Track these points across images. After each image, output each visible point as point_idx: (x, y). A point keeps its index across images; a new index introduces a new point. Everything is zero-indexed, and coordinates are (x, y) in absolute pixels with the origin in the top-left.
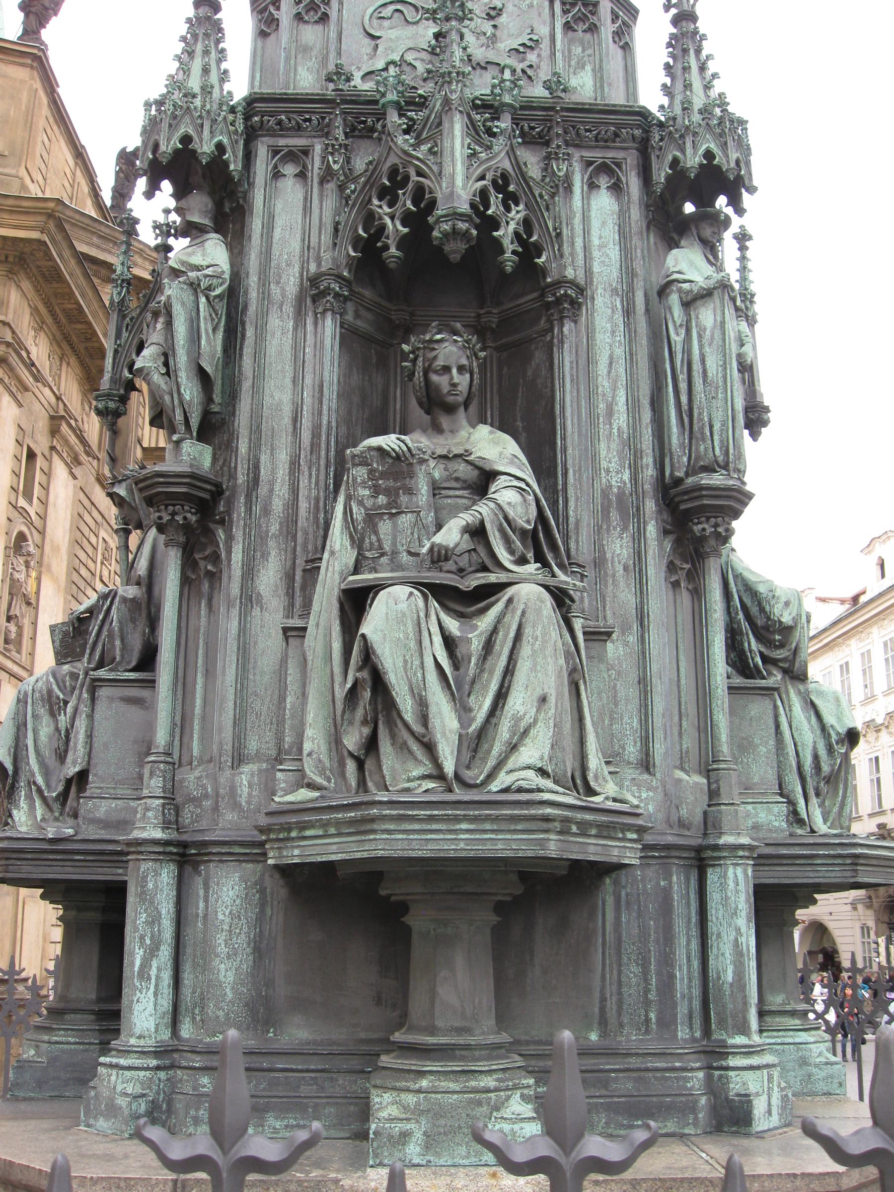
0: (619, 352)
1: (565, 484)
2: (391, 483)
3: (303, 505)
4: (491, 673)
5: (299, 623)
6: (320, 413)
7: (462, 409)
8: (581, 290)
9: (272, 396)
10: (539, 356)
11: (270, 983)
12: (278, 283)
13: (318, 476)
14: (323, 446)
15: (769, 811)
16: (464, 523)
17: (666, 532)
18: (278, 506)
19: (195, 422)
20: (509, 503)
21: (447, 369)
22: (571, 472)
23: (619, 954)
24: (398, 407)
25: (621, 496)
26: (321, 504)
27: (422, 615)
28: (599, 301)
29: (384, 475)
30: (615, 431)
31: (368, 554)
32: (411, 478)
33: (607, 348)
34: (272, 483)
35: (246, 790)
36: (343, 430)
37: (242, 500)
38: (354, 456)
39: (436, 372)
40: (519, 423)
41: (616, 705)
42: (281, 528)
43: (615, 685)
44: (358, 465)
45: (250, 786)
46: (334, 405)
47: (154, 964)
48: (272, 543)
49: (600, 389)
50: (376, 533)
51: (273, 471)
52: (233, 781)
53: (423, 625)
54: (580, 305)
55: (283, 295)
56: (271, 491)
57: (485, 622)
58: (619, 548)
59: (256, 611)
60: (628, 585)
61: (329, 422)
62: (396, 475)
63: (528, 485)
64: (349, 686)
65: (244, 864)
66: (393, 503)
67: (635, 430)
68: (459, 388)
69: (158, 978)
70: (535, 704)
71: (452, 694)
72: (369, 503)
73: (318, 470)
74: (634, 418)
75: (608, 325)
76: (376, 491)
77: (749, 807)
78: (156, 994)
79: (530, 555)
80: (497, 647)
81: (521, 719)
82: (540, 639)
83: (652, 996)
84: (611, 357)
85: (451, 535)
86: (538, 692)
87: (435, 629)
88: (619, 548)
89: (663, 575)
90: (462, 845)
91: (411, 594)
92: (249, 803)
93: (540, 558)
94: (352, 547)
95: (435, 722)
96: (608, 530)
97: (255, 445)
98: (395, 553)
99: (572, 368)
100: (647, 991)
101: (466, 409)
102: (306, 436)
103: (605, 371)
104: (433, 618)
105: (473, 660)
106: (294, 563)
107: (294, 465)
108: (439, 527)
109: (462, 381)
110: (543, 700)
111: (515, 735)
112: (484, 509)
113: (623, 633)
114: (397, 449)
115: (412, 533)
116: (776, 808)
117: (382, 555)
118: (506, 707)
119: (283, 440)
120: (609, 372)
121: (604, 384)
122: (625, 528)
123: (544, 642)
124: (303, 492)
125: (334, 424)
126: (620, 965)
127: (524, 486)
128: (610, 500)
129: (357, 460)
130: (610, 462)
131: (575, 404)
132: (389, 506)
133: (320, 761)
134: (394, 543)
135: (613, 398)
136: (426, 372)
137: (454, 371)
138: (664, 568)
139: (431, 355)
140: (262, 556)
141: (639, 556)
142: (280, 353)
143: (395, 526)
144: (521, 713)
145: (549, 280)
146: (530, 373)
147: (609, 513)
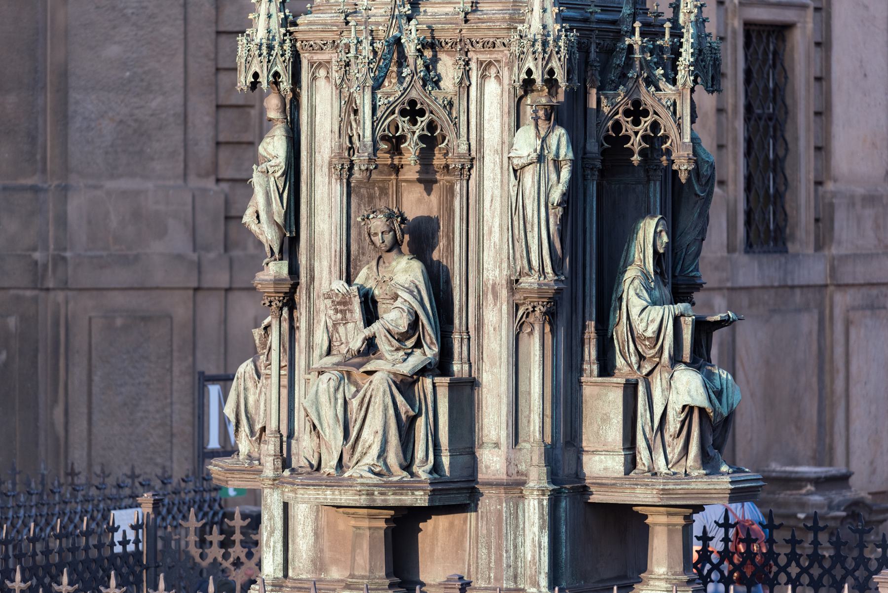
0: (497, 192)
2: (342, 307)
11: (321, 551)
15: (614, 460)
19: (276, 250)
23: (477, 543)
34: (321, 279)
47: (272, 539)
51: (321, 272)
56: (321, 284)
62: (344, 303)
66: (344, 318)
69: (274, 547)
72: (334, 318)
76: (337, 311)
77: (603, 457)
78: (273, 555)
83: (492, 565)
84: (492, 197)
86: (375, 429)
100: (490, 562)
116: (617, 458)
122: (495, 304)
126: (477, 548)
132: (342, 320)
134: (347, 338)
142: (322, 199)
143: (346, 329)
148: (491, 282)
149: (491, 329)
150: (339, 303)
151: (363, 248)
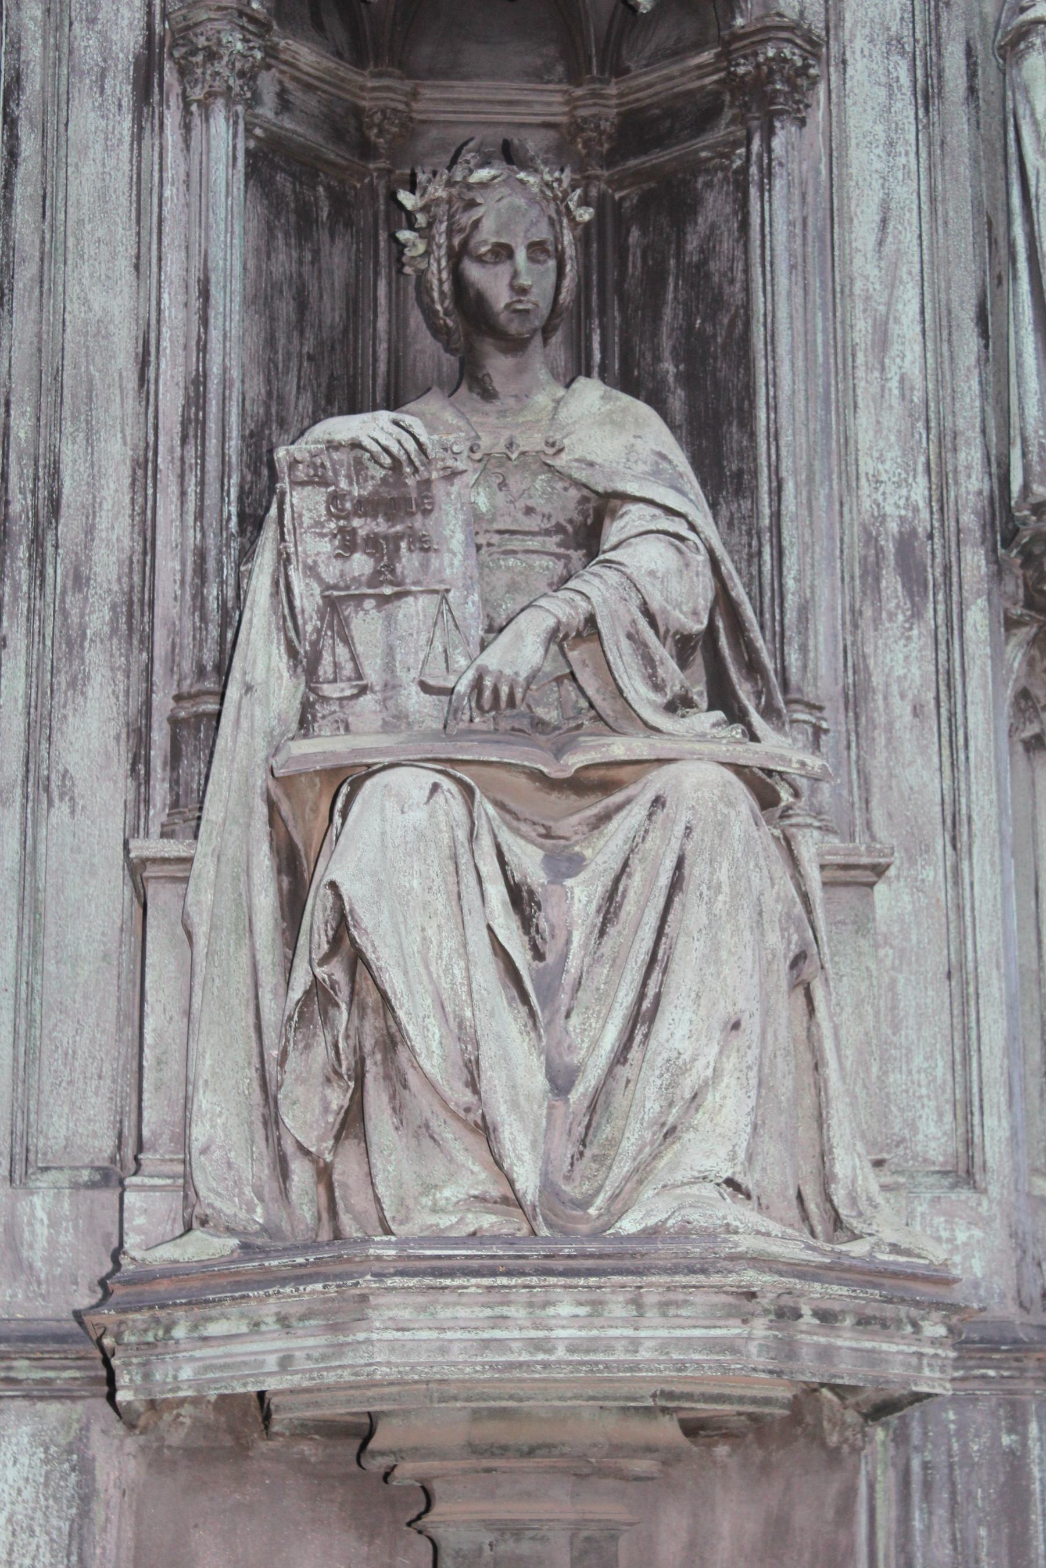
0: (905, 193)
1: (777, 516)
2: (381, 526)
3: (169, 568)
4: (617, 963)
5: (173, 848)
6: (203, 348)
7: (538, 340)
8: (814, 46)
9: (86, 301)
10: (715, 205)
12: (92, 21)
13: (201, 497)
14: (212, 426)
16: (551, 622)
17: (1011, 624)
18: (107, 566)
20: (652, 573)
21: (503, 252)
22: (789, 488)
24: (382, 323)
25: (906, 543)
26: (211, 565)
27: (462, 835)
28: (858, 69)
29: (366, 507)
30: (894, 384)
31: (327, 690)
32: (426, 513)
33: (877, 185)
34: (91, 511)
35: (43, 1231)
36: (256, 387)
37: (22, 552)
38: (294, 463)
39: (480, 259)
40: (669, 367)
41: (896, 1029)
42: (115, 619)
43: (893, 982)
44: (303, 484)
45: (54, 1223)
46: (235, 330)
48: (94, 655)
49: (858, 285)
50: (347, 641)
51: (93, 484)
52: (13, 1213)
53: (464, 859)
54: (814, 81)
55: (106, 53)
56: (90, 530)
57: (603, 853)
58: (901, 660)
59: (61, 811)
60: (923, 750)
61: (225, 370)
63: (692, 527)
64: (297, 994)
65: (40, 1406)
66: (385, 571)
67: (939, 382)
68: (532, 297)
70: (717, 1035)
71: (532, 1014)
72: (330, 572)
73: (202, 483)
74: (938, 354)
75: (879, 128)
76: (348, 543)
79: (699, 692)
80: (629, 908)
81: (684, 1070)
82: (726, 889)
85: (521, 652)
86: (724, 1010)
87: (490, 867)
88: (901, 660)
89: (1004, 724)
90: (560, 1354)
91: (435, 787)
92: (50, 1261)
93: (722, 697)
94: (294, 673)
95: (492, 1078)
96: (877, 621)
97: (49, 422)
98: (391, 687)
99: (791, 236)
101: (545, 341)
102: (171, 400)
103: (872, 239)
104: (486, 843)
105: (577, 938)
106: (148, 703)
107: (144, 467)
108: (494, 630)
109: (538, 280)
110: (736, 1026)
111: (671, 1104)
112: (597, 588)
113: (912, 860)
114: (395, 448)
115: (430, 642)
117: (363, 690)
118: (653, 1043)
119: (115, 409)
120: (881, 243)
121: (865, 268)
122: (917, 614)
123: (735, 895)
124: (167, 534)
125: (235, 373)
127: (683, 530)
128: (880, 551)
129: (301, 472)
130: (881, 459)
131: (799, 324)
132: (375, 579)
133: (230, 1165)
134: (389, 667)
135: (889, 305)
136: (456, 257)
137: (521, 255)
138: (1006, 709)
139: (465, 219)
140: (72, 684)
141: (948, 680)
142: (103, 196)
143: (390, 621)
144: (686, 1056)
145: (739, 21)
146: (692, 244)
147: (877, 580)
148: (893, 527)
149: (903, 710)
150: (366, 507)
151: (281, 400)
